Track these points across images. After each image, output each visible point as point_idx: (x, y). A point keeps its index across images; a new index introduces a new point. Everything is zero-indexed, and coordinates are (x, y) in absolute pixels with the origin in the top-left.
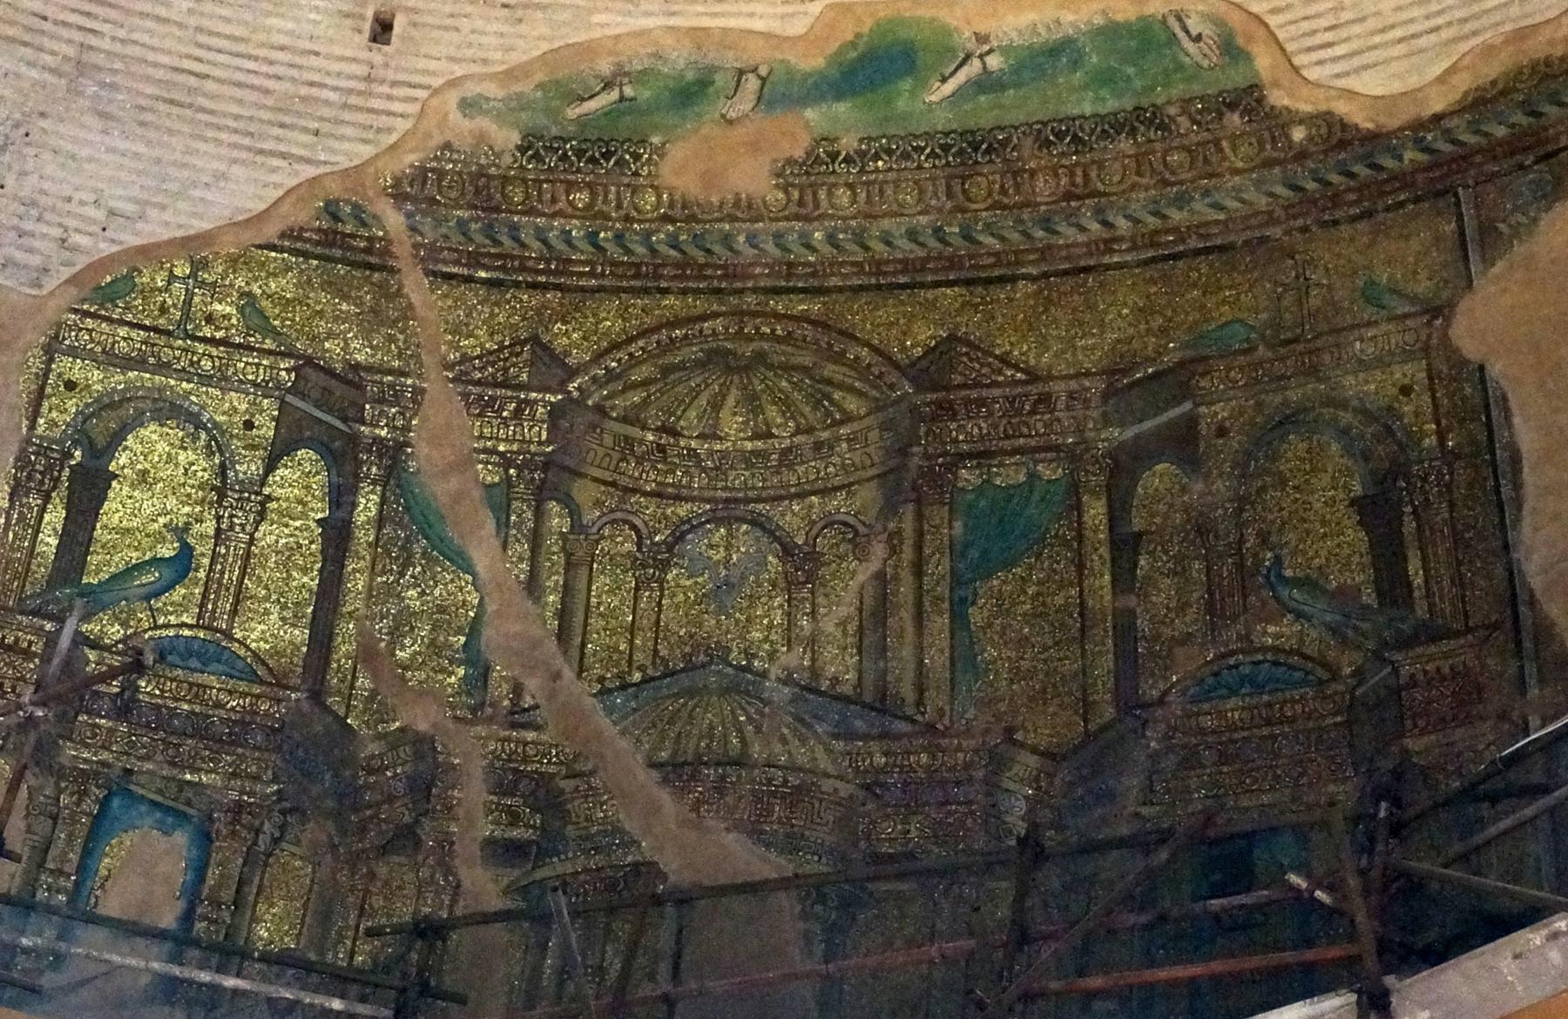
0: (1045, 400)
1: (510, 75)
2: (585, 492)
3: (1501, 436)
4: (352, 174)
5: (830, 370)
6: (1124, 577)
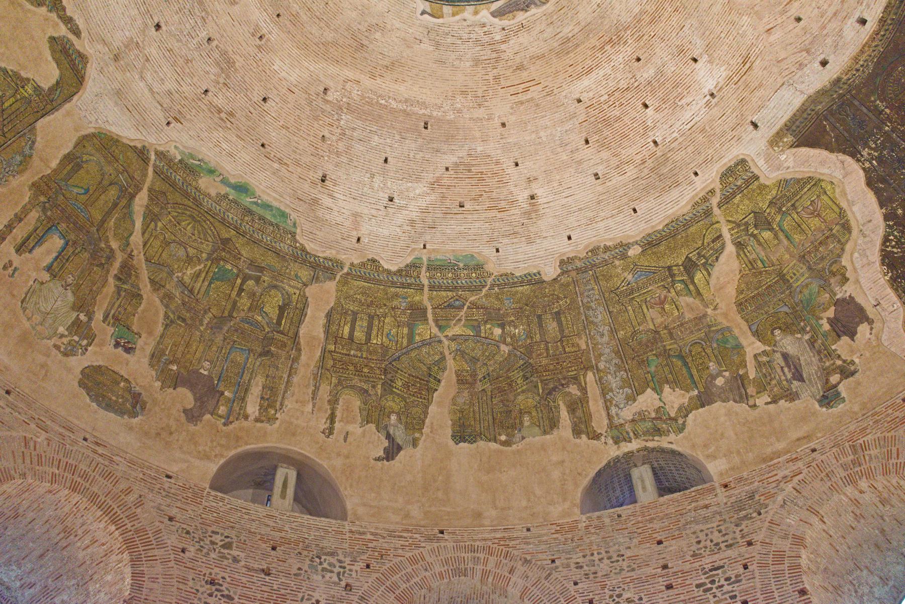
0: (240, 258)
1: (184, 147)
2: (160, 224)
3: (305, 310)
4: (151, 144)
5: (209, 231)
6: (239, 294)
